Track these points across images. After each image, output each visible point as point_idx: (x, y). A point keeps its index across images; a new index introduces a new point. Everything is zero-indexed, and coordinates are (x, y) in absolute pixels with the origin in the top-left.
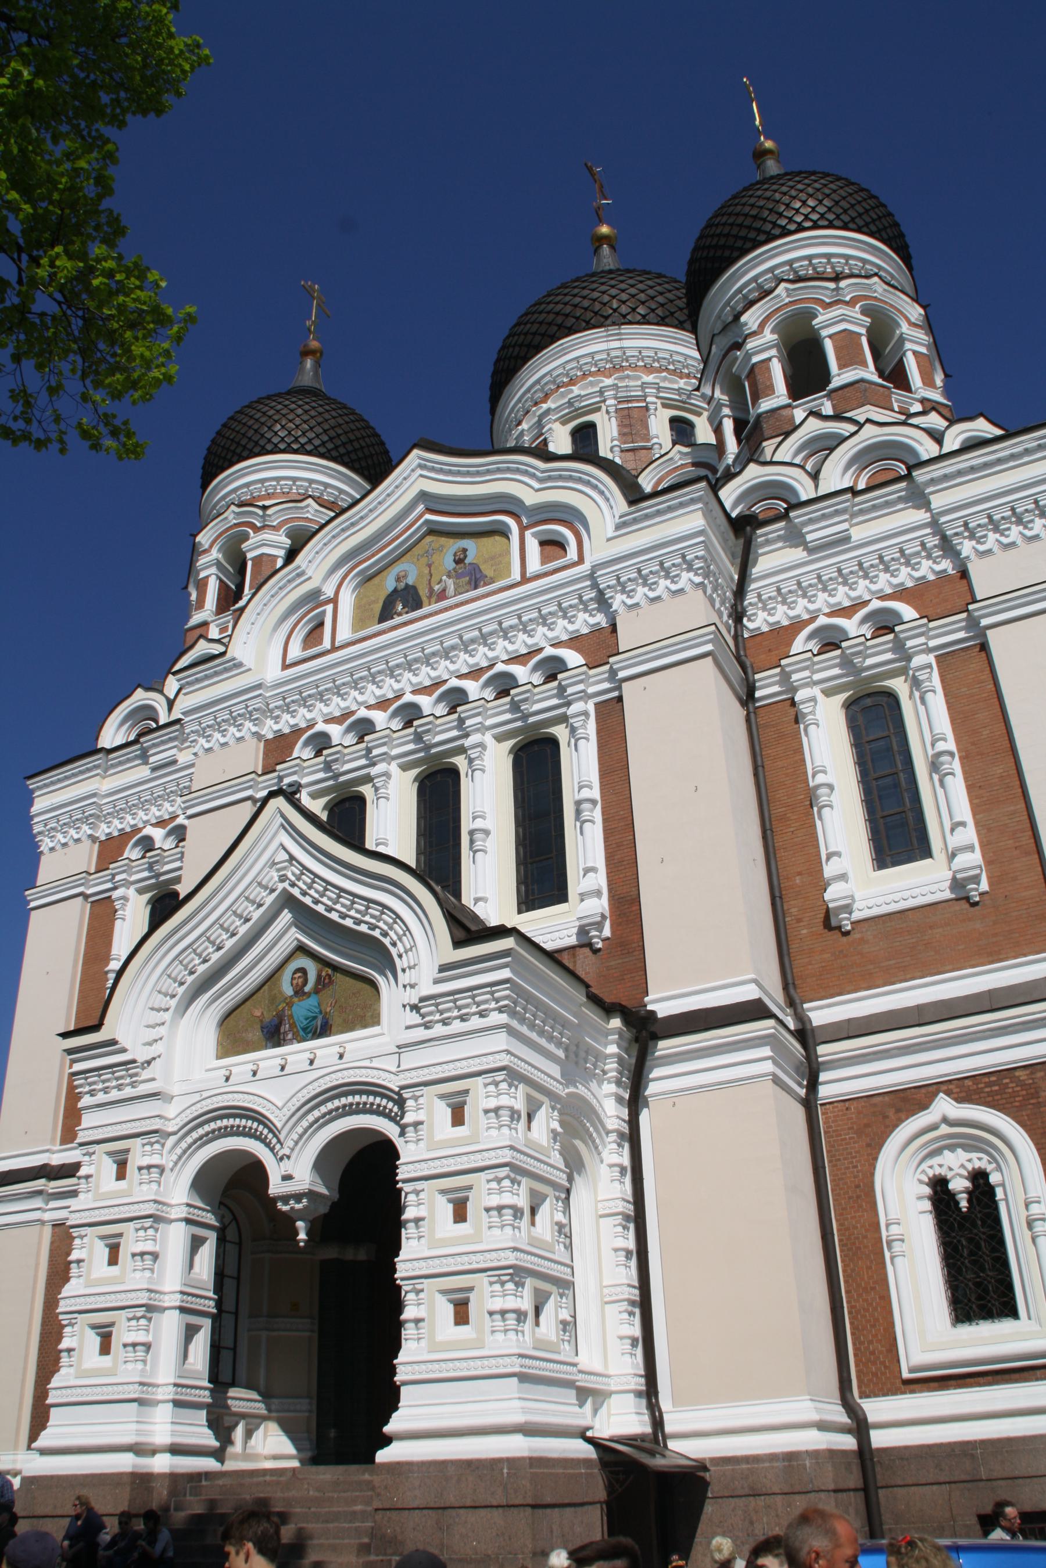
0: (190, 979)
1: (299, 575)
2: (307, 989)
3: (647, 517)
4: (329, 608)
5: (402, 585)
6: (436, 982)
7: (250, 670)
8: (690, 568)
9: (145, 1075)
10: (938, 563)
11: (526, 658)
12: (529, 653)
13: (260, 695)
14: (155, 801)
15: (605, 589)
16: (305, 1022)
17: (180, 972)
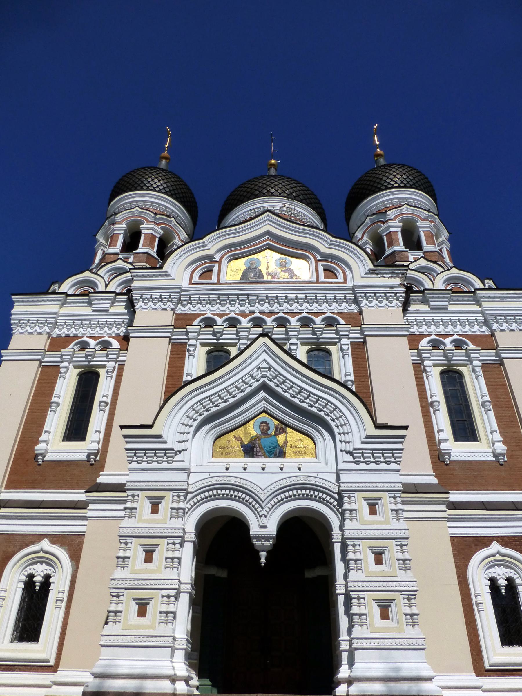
0: (206, 414)
1: (203, 246)
2: (269, 432)
4: (217, 265)
6: (363, 442)
7: (174, 279)
8: (397, 299)
9: (177, 458)
11: (316, 314)
13: (179, 292)
14: (90, 325)
15: (359, 297)
17: (201, 409)
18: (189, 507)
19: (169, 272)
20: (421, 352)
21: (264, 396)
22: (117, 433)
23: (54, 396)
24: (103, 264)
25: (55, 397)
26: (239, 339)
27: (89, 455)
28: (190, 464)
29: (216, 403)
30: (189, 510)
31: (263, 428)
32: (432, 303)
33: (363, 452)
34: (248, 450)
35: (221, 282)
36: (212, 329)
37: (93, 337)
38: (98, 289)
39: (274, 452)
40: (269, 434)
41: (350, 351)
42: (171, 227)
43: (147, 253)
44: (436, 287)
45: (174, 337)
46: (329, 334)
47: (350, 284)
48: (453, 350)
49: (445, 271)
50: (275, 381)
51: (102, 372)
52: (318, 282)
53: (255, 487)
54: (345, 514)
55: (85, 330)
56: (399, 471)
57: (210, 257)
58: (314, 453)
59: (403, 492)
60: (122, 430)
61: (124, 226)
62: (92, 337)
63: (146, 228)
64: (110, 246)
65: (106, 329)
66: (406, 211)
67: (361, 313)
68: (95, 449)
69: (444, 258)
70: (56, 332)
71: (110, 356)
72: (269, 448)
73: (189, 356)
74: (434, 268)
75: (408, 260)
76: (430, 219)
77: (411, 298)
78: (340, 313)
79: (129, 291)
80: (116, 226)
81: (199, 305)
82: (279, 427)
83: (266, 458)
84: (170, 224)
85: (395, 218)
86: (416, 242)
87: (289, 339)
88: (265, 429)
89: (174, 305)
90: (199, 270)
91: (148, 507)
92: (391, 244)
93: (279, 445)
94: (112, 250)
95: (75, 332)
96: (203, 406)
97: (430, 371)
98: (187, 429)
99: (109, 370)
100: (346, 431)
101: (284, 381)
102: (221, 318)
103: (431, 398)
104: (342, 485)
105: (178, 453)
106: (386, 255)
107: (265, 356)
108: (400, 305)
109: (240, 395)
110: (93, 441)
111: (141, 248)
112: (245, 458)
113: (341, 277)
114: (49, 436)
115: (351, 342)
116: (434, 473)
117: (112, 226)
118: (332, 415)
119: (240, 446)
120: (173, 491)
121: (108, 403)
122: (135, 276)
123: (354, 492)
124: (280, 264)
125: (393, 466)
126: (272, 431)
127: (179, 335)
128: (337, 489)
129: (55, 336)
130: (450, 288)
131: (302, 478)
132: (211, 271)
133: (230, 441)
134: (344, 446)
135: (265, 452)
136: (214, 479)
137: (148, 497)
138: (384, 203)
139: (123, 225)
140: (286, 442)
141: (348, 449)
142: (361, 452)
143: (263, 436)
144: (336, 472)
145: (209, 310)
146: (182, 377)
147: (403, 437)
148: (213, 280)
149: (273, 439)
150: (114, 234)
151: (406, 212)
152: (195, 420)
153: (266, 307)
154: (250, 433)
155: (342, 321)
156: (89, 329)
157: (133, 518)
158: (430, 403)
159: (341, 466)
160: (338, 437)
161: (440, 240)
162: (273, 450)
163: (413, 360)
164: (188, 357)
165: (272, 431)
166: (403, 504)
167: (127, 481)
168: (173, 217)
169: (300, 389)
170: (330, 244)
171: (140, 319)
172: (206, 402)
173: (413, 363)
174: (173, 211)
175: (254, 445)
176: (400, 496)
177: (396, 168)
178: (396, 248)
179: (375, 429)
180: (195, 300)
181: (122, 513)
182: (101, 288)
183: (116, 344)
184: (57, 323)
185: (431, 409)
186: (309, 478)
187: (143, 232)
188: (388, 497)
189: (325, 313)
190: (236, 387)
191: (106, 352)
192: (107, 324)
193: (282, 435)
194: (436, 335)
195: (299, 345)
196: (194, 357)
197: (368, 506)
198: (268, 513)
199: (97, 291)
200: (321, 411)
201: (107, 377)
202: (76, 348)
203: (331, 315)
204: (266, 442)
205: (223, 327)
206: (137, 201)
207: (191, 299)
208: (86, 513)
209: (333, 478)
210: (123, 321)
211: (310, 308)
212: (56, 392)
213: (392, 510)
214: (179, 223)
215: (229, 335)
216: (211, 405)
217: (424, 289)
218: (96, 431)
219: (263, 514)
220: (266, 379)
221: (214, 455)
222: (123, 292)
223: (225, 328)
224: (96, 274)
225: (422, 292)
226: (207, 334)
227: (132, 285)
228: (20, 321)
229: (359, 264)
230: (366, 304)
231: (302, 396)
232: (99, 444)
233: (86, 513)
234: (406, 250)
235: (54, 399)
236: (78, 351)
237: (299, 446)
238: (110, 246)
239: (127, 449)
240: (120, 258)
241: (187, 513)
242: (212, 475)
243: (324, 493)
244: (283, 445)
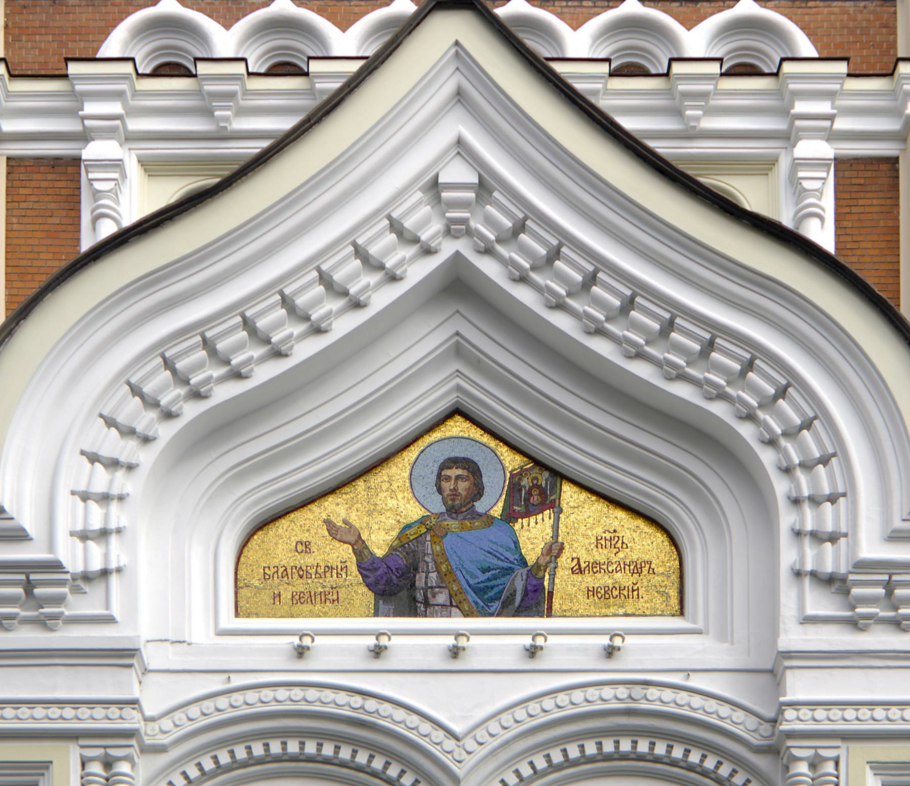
2: (480, 506)
16: (483, 577)
31: (455, 489)
34: (389, 582)
39: (501, 592)
40: (480, 515)
53: (426, 727)
58: (673, 593)
72: (479, 573)
82: (526, 482)
83: (466, 615)
88: (464, 493)
93: (523, 562)
104: (790, 714)
112: (376, 614)
119: (354, 568)
120: (82, 742)
131: (622, 692)
135: (461, 591)
136: (251, 696)
140: (554, 550)
143: (453, 524)
162: (499, 581)
186: (653, 692)
193: (540, 517)
242: (238, 681)
244: (542, 562)
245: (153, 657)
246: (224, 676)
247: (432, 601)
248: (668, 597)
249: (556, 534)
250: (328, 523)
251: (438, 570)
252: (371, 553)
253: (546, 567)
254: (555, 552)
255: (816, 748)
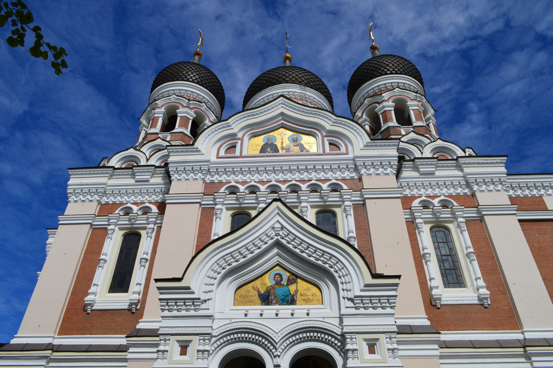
0: (228, 268)
1: (228, 126)
2: (282, 283)
3: (376, 146)
4: (239, 142)
5: (270, 142)
6: (362, 291)
7: (204, 154)
8: (391, 167)
9: (203, 306)
10: (464, 190)
12: (325, 180)
13: (208, 165)
14: (134, 194)
15: (359, 166)
16: (282, 297)
17: (224, 263)
18: (213, 349)
19: (200, 148)
20: (413, 211)
21: (278, 251)
22: (153, 285)
23: (102, 254)
24: (145, 142)
25: (103, 255)
26: (258, 204)
27: (131, 304)
28: (214, 311)
29: (237, 258)
30: (213, 351)
31: (277, 280)
32: (421, 170)
33: (363, 299)
34: (264, 298)
35: (243, 156)
36: (235, 196)
37: (135, 203)
38: (140, 164)
39: (286, 300)
40: (282, 284)
41: (352, 212)
42: (203, 111)
43: (182, 133)
44: (424, 156)
45: (203, 203)
46: (334, 198)
47: (351, 156)
48: (441, 209)
49: (432, 142)
50: (287, 238)
51: (143, 233)
52: (324, 154)
54: (348, 353)
55: (129, 197)
56: (394, 315)
57: (235, 135)
58: (321, 301)
59: (398, 333)
60: (156, 283)
61: (163, 110)
62: (136, 204)
63: (181, 112)
64: (151, 127)
65: (147, 197)
66: (398, 93)
67: (360, 179)
68: (136, 300)
69: (431, 132)
70: (104, 200)
71: (150, 220)
72: (282, 296)
73: (216, 218)
74: (423, 140)
75: (400, 134)
76: (418, 100)
77: (403, 166)
78: (344, 180)
79: (166, 165)
80: (156, 111)
81: (225, 176)
82: (291, 278)
84: (201, 109)
85: (389, 99)
86: (407, 118)
87: (300, 203)
89: (204, 176)
90: (225, 147)
91: (178, 349)
92: (386, 121)
93: (290, 294)
94: (153, 131)
95: (120, 200)
96: (225, 261)
97: (422, 228)
98: (212, 281)
99: (149, 232)
100: (347, 281)
101: (294, 239)
102: (243, 186)
103: (423, 250)
104: (345, 328)
105: (204, 302)
106: (382, 130)
107: (278, 218)
108: (395, 172)
109: (257, 252)
110: (134, 293)
111: (177, 129)
112: (261, 305)
113: (343, 150)
114: (97, 289)
115: (353, 204)
116: (427, 316)
117: (153, 111)
118: (335, 267)
119: (257, 296)
121: (148, 260)
122: (170, 152)
123: (356, 334)
124: (293, 140)
125: (389, 310)
126: (284, 282)
127: (208, 201)
128: (341, 332)
129: (104, 203)
130: (436, 157)
132: (235, 147)
133: (248, 291)
134: (346, 294)
135: (278, 300)
136: (235, 324)
137: (178, 341)
138: (379, 87)
139: (162, 110)
140: (297, 291)
141: (349, 297)
142: (361, 299)
143: (277, 286)
144: (338, 316)
145: (233, 179)
146: (210, 237)
147: (397, 285)
148: (236, 154)
149: (285, 288)
150: (155, 117)
151: (398, 94)
152: (219, 273)
153: (281, 177)
154: (266, 284)
155: (345, 187)
156: (133, 197)
157: (165, 360)
158: (422, 254)
159: (344, 311)
160: (340, 286)
161: (428, 116)
163: (406, 218)
164: (216, 220)
165: (284, 282)
166: (398, 344)
167: (160, 327)
168: (204, 102)
169: (308, 245)
170: (334, 122)
171: (175, 188)
172: (229, 258)
173: (406, 221)
174: (204, 97)
175: (270, 294)
176: (395, 337)
177: (389, 58)
178: (390, 124)
179: (372, 279)
180: (221, 171)
181: (155, 356)
182: (143, 162)
183: (154, 209)
184: (106, 192)
185: (424, 261)
187: (179, 115)
188: (385, 338)
189: (330, 180)
190: (254, 244)
191: (146, 216)
192: (148, 193)
193: (293, 285)
194: (426, 197)
195: (309, 207)
196: (220, 219)
197: (367, 346)
198: (281, 353)
199: (140, 165)
200: (326, 263)
201: (147, 237)
202: (121, 213)
203: (335, 181)
204: (280, 291)
205: (245, 193)
206: (174, 90)
207: (218, 170)
208: (126, 356)
209: (336, 322)
210: (161, 190)
211: (318, 176)
212: (104, 250)
213: (389, 350)
214: (209, 107)
215: (250, 200)
216: (232, 260)
217: (414, 158)
218: (138, 284)
219: (277, 355)
220: (279, 237)
221: (235, 303)
222: (162, 165)
223: (246, 194)
224: (139, 150)
225: (413, 160)
226: (231, 200)
227: (168, 160)
228: (75, 190)
229: (359, 139)
230: (365, 172)
231: (309, 251)
232: (139, 295)
233: (126, 356)
234: (399, 125)
235: (102, 257)
236: (123, 215)
237: (308, 295)
238: (151, 127)
239: (160, 299)
240: (159, 137)
241: (211, 354)
243: (329, 335)
244: (294, 294)
245: (216, 317)
246: (230, 320)
247: (272, 302)
248: (320, 301)
249: (297, 288)
250: (253, 287)
251: (274, 296)
252: (261, 292)
253: (295, 295)
254: (297, 292)
255: (351, 335)
